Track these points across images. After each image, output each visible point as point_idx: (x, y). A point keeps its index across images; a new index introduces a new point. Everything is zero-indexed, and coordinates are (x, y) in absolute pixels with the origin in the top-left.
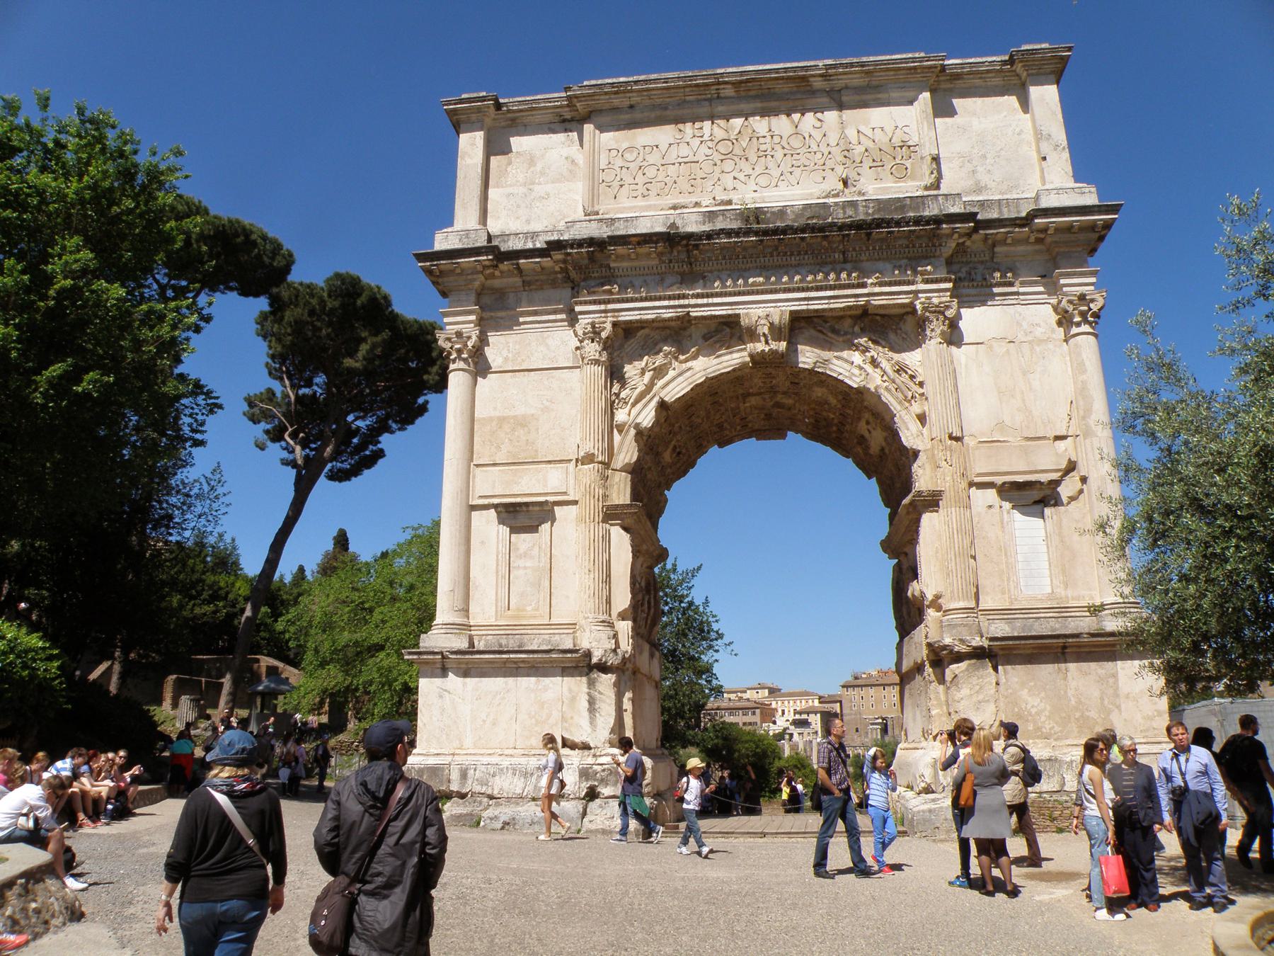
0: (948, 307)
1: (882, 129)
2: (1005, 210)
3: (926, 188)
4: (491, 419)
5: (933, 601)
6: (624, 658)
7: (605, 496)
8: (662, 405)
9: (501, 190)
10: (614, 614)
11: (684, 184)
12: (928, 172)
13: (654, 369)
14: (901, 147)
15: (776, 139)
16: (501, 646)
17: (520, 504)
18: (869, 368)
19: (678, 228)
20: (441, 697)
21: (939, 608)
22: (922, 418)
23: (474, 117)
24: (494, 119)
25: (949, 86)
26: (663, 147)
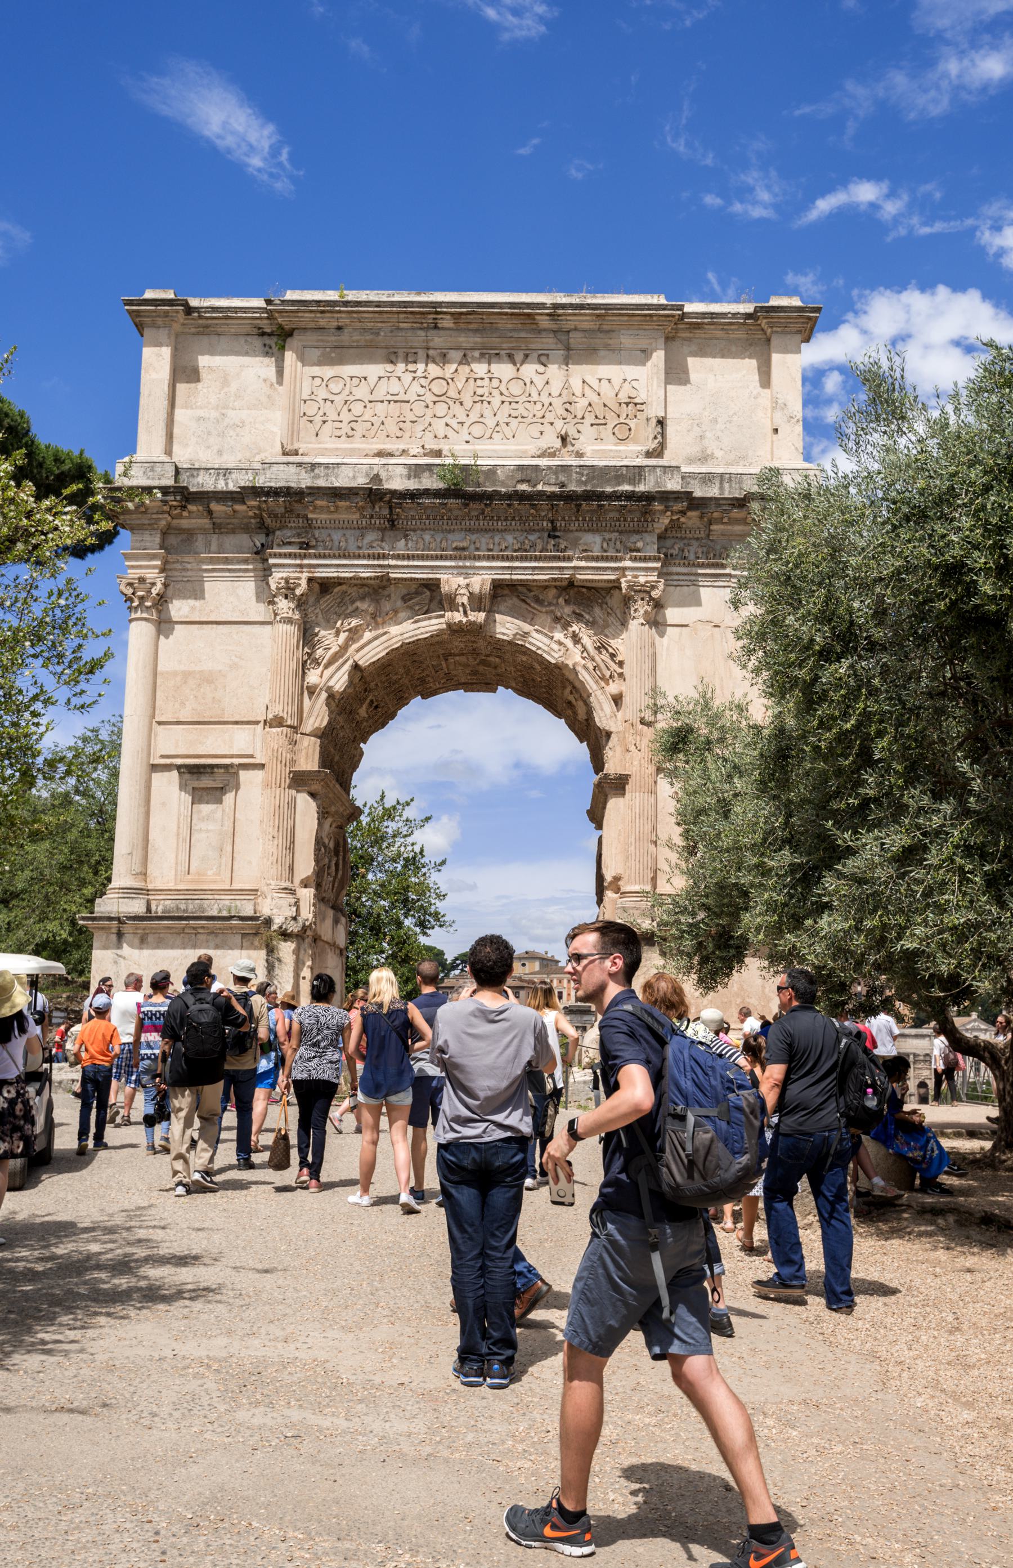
0: (653, 587)
1: (609, 380)
2: (726, 485)
3: (649, 454)
4: (175, 674)
5: (610, 883)
6: (304, 925)
7: (293, 762)
8: (356, 667)
9: (189, 412)
10: (297, 881)
11: (392, 427)
12: (651, 436)
13: (349, 630)
14: (627, 404)
15: (495, 383)
16: (178, 908)
17: (204, 766)
18: (569, 643)
19: (381, 480)
20: (116, 962)
21: (617, 890)
22: (617, 700)
23: (160, 321)
24: (183, 324)
25: (688, 335)
26: (372, 380)
